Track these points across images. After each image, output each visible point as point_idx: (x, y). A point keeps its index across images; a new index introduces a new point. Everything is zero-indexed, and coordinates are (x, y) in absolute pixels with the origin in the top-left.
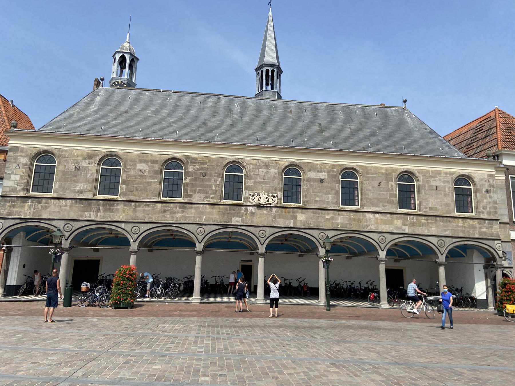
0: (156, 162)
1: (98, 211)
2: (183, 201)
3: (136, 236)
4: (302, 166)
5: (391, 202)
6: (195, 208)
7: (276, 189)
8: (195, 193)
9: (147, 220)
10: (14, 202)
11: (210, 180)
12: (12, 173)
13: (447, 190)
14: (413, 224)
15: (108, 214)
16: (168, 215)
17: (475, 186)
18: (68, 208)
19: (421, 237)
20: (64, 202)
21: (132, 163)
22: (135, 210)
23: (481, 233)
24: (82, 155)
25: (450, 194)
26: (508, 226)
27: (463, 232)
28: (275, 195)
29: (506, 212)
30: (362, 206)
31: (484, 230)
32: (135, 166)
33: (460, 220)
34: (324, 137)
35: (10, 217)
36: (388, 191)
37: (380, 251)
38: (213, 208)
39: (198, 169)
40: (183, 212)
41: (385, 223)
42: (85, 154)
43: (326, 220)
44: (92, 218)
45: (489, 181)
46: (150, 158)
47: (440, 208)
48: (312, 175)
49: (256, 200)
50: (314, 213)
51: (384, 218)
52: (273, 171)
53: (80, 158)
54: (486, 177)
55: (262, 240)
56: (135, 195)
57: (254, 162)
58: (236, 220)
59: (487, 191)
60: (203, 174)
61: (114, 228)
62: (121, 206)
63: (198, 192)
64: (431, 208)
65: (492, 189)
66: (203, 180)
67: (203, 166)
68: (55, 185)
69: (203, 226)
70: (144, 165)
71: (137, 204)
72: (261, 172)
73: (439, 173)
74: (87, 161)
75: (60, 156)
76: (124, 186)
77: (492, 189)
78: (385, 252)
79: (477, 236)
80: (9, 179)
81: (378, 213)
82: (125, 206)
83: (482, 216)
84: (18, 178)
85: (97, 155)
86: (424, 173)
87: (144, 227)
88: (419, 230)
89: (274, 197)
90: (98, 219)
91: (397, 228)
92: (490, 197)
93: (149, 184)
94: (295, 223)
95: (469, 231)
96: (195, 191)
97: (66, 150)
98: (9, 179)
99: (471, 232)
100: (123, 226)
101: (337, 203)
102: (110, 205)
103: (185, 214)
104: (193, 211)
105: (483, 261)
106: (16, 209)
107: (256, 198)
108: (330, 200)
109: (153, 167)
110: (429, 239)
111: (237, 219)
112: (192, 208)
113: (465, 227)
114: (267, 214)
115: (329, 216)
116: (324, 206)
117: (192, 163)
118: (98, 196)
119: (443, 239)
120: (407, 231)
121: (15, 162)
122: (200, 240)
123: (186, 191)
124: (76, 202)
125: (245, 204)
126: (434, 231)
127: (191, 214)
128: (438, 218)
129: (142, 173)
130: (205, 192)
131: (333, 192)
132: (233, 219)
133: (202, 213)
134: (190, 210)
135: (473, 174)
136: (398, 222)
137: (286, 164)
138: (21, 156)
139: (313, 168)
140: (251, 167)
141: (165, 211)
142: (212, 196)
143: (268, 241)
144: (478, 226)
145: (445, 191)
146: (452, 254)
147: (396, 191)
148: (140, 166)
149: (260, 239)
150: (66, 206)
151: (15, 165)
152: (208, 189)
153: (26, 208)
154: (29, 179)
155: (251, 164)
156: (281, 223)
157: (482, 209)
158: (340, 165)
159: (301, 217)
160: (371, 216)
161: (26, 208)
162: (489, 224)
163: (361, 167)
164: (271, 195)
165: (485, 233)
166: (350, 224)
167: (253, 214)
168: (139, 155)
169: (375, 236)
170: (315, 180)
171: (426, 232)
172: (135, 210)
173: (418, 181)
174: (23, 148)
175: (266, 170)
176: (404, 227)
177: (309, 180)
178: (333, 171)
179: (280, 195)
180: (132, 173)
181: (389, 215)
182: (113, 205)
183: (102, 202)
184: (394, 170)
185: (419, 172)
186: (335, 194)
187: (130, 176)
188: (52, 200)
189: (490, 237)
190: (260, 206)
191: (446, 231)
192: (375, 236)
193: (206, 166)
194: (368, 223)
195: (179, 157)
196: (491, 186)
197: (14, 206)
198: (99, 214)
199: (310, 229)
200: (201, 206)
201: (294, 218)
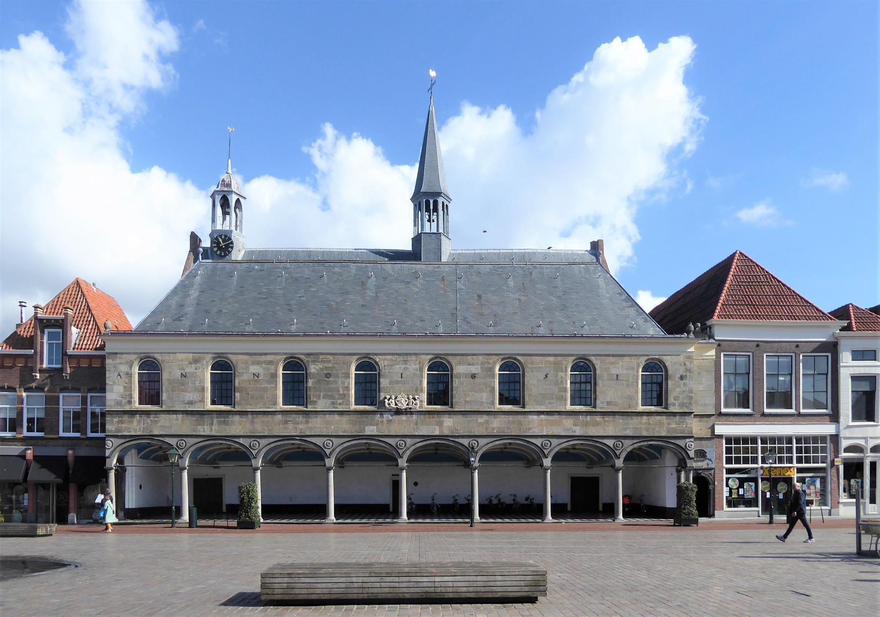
1: (212, 424)
8: (319, 398)
11: (336, 382)
12: (114, 383)
13: (631, 380)
15: (223, 427)
16: (290, 426)
21: (243, 366)
22: (252, 422)
27: (647, 429)
28: (416, 397)
31: (674, 426)
32: (247, 369)
39: (322, 369)
40: (307, 422)
44: (207, 433)
47: (620, 402)
59: (682, 378)
60: (328, 375)
62: (237, 418)
64: (609, 403)
65: (688, 374)
66: (328, 383)
67: (327, 365)
68: (164, 396)
69: (332, 439)
77: (688, 374)
79: (664, 434)
80: (112, 391)
83: (672, 409)
88: (593, 431)
89: (415, 399)
90: (213, 433)
92: (685, 385)
98: (112, 391)
99: (657, 429)
100: (241, 441)
103: (310, 425)
106: (124, 425)
108: (484, 400)
109: (268, 369)
111: (371, 428)
113: (649, 424)
115: (481, 419)
120: (577, 433)
126: (611, 430)
130: (331, 397)
138: (121, 363)
141: (286, 422)
142: (339, 401)
145: (628, 381)
146: (631, 457)
150: (177, 420)
152: (335, 393)
153: (135, 423)
156: (424, 431)
161: (135, 423)
165: (674, 430)
167: (389, 421)
169: (538, 442)
170: (466, 375)
172: (252, 422)
175: (404, 366)
176: (574, 428)
187: (243, 381)
190: (398, 412)
191: (625, 429)
192: (538, 442)
194: (530, 426)
196: (687, 370)
197: (122, 422)
198: (213, 428)
201: (440, 424)
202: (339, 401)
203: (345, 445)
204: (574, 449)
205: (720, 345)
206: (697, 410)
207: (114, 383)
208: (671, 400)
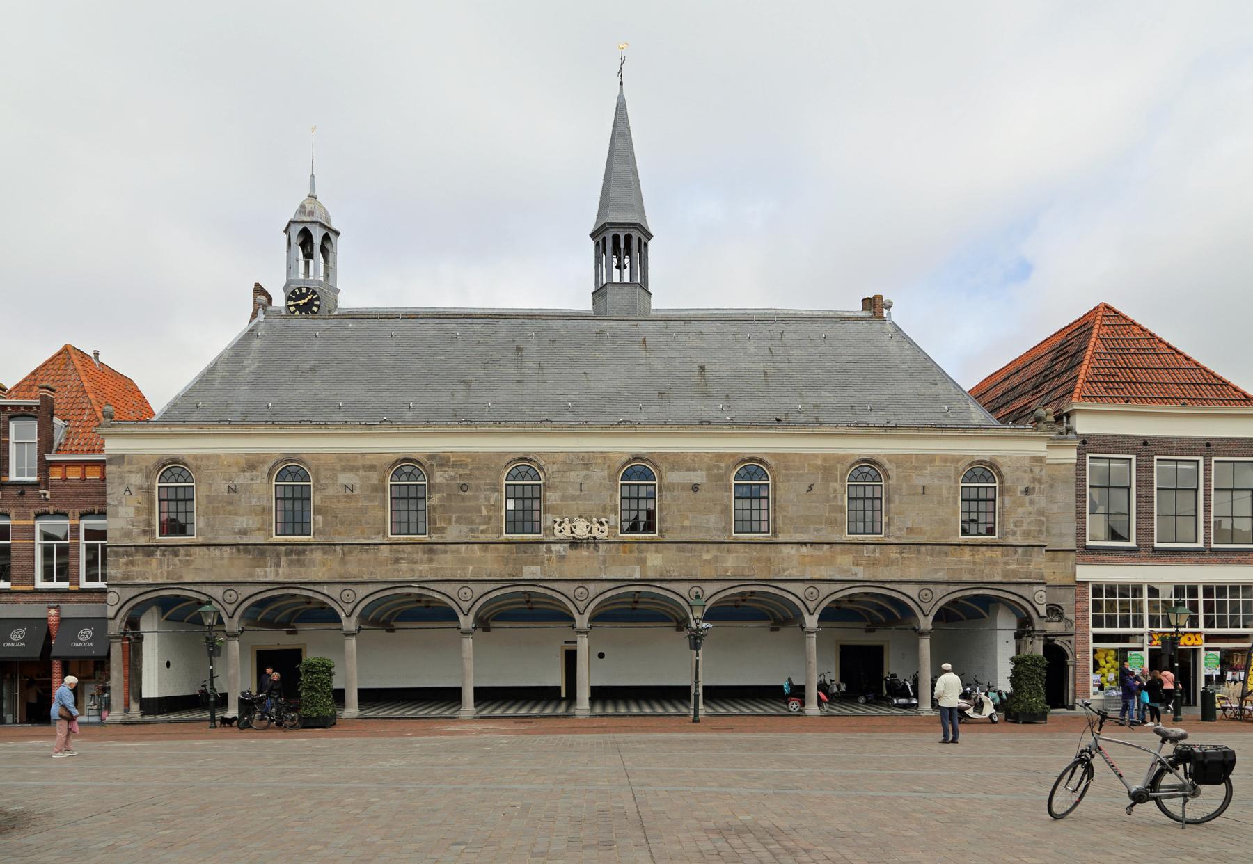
0: (372, 468)
2: (429, 540)
3: (350, 606)
4: (657, 461)
5: (832, 523)
6: (452, 552)
7: (604, 509)
8: (450, 523)
9: (366, 578)
10: (131, 555)
11: (476, 498)
12: (120, 503)
13: (945, 492)
15: (295, 569)
16: (404, 566)
17: (1002, 482)
18: (225, 562)
20: (216, 552)
21: (328, 473)
22: (343, 561)
23: (1005, 574)
24: (237, 463)
25: (951, 500)
26: (1073, 555)
27: (971, 572)
28: (603, 520)
29: (1072, 529)
30: (775, 533)
31: (1014, 566)
33: (967, 549)
34: (707, 395)
35: (129, 582)
36: (827, 500)
37: (806, 616)
38: (486, 550)
39: (453, 478)
40: (431, 560)
41: (819, 562)
42: (243, 462)
43: (704, 562)
44: (271, 578)
45: (1031, 471)
46: (360, 462)
48: (674, 477)
49: (567, 533)
50: (679, 550)
52: (599, 474)
53: (235, 469)
54: (1027, 463)
55: (581, 605)
56: (340, 534)
57: (561, 458)
58: (531, 572)
61: (309, 594)
62: (317, 555)
63: (457, 522)
64: (910, 530)
65: (1037, 486)
66: (463, 499)
67: (461, 471)
69: (469, 585)
70: (350, 475)
71: (346, 548)
72: (575, 476)
73: (931, 459)
74: (248, 474)
75: (198, 468)
76: (319, 518)
77: (1037, 486)
78: (816, 616)
79: (998, 579)
80: (116, 515)
81: (805, 543)
82: (325, 553)
83: (1011, 540)
84: (131, 512)
85: (264, 462)
87: (362, 591)
88: (883, 574)
89: (601, 523)
90: (281, 579)
92: (1032, 502)
93: (364, 510)
94: (643, 572)
96: (449, 521)
97: (208, 457)
98: (116, 515)
99: (987, 571)
100: (325, 589)
101: (726, 530)
102: (299, 553)
103: (435, 565)
104: (449, 557)
105: (1014, 624)
106: (136, 569)
107: (567, 526)
108: (711, 525)
109: (368, 478)
110: (904, 588)
111: (533, 568)
112: (446, 552)
113: (974, 563)
114: (589, 558)
116: (701, 538)
117: (441, 466)
118: (276, 539)
119: (931, 587)
120: (860, 576)
121: (121, 484)
122: (465, 609)
123: (432, 521)
124: (239, 550)
125: (546, 539)
126: (913, 573)
127: (446, 564)
128: (923, 549)
129: (348, 492)
130: (470, 521)
131: (719, 508)
132: (525, 569)
133: (464, 561)
134: (443, 556)
135: (999, 459)
137: (624, 459)
138: (130, 472)
139: (677, 461)
140: (555, 467)
141: (397, 561)
142: (482, 527)
143: (592, 606)
144: (1000, 559)
147: (842, 500)
148: (344, 478)
149: (578, 603)
150: (222, 558)
151: (122, 489)
152: (474, 516)
154: (151, 513)
155: (554, 463)
156: (617, 572)
157: (1012, 526)
158: (732, 455)
159: (656, 562)
160: (790, 550)
162: (1025, 554)
163: (774, 456)
164: (595, 520)
165: (1014, 572)
166: (751, 568)
167: (562, 558)
168: (340, 457)
169: (798, 589)
170: (683, 487)
171: (898, 577)
172: (343, 561)
173: (888, 478)
174: (131, 457)
175: (584, 473)
176: (855, 569)
177: (671, 487)
178: (718, 468)
179: (615, 519)
180: (331, 491)
181: (826, 547)
182: (303, 552)
183: (283, 548)
184: (840, 459)
185: (890, 461)
186: (722, 512)
187: (327, 498)
188: (197, 549)
190: (575, 544)
192: (798, 589)
193: (467, 471)
195: (414, 457)
196: (1034, 480)
197: (132, 563)
198: (281, 571)
200: (464, 547)
201: (642, 562)
202: (482, 527)
203: (491, 596)
204: (850, 601)
205: (1086, 443)
206: (1052, 543)
207: (120, 503)
208: (1010, 526)
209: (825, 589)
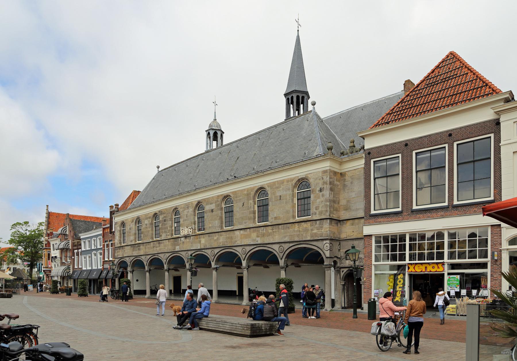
0: (150, 217)
14: (263, 235)
19: (268, 246)
27: (298, 236)
31: (315, 231)
33: (296, 224)
41: (246, 236)
45: (323, 178)
50: (209, 236)
51: (246, 233)
54: (320, 175)
58: (177, 248)
59: (321, 190)
60: (165, 221)
64: (276, 218)
73: (282, 182)
77: (325, 186)
79: (309, 238)
81: (242, 229)
86: (272, 185)
91: (254, 240)
92: (323, 196)
94: (200, 246)
95: (302, 235)
99: (304, 235)
120: (259, 242)
126: (277, 239)
128: (280, 226)
136: (254, 235)
139: (208, 201)
144: (310, 228)
145: (286, 199)
148: (146, 222)
165: (315, 234)
181: (248, 230)
184: (252, 189)
185: (268, 186)
189: (319, 238)
190: (186, 237)
191: (285, 237)
199: (206, 249)
201: (200, 242)
209: (248, 248)
